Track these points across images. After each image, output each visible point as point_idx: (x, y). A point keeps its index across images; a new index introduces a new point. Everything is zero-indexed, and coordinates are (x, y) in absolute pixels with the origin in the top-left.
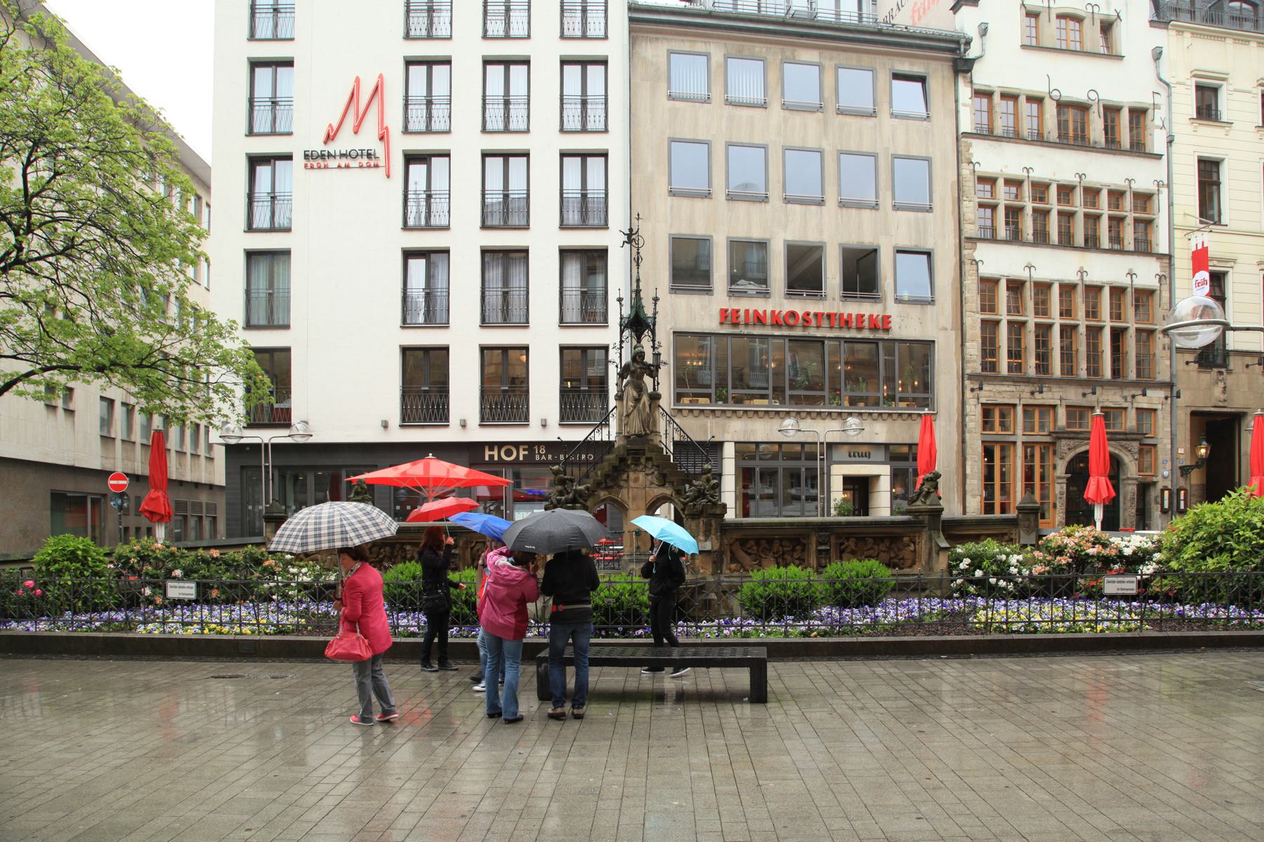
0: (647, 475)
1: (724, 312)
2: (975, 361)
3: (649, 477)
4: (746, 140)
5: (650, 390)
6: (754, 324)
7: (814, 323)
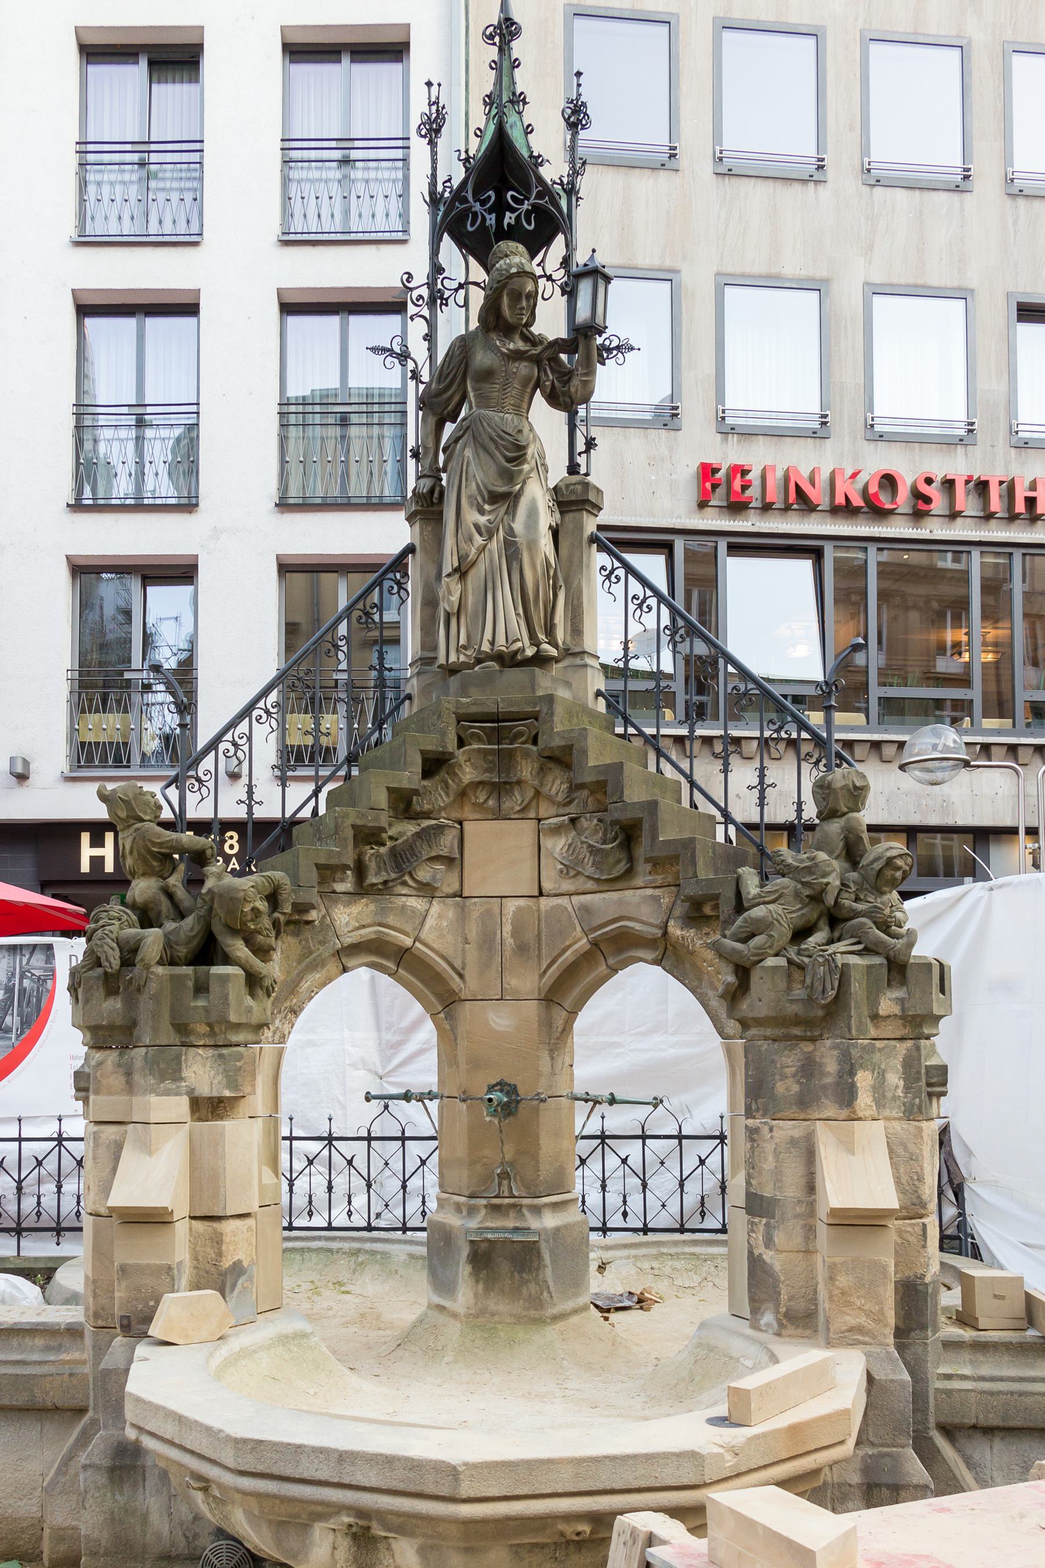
1: (707, 471)
4: (766, 15)
5: (558, 473)
6: (787, 508)
7: (939, 504)
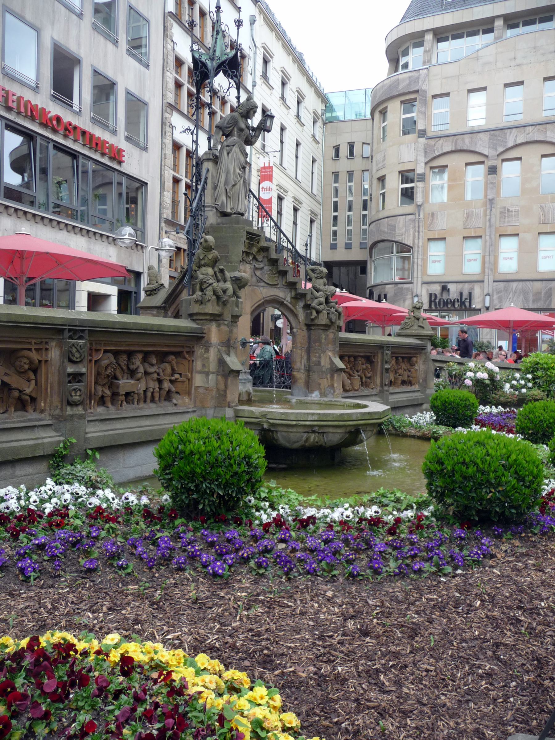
0: (257, 269)
2: (168, 209)
3: (258, 273)
